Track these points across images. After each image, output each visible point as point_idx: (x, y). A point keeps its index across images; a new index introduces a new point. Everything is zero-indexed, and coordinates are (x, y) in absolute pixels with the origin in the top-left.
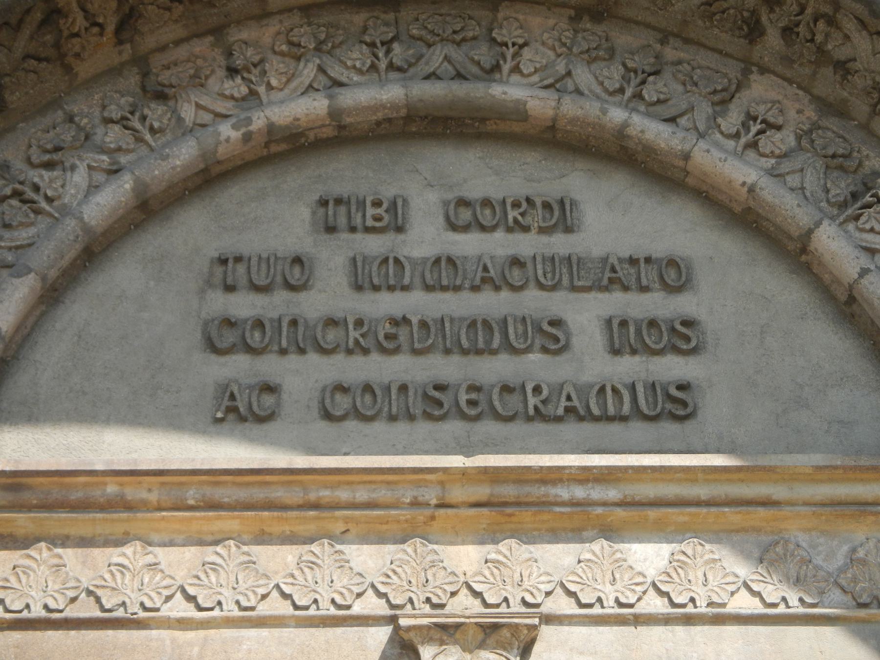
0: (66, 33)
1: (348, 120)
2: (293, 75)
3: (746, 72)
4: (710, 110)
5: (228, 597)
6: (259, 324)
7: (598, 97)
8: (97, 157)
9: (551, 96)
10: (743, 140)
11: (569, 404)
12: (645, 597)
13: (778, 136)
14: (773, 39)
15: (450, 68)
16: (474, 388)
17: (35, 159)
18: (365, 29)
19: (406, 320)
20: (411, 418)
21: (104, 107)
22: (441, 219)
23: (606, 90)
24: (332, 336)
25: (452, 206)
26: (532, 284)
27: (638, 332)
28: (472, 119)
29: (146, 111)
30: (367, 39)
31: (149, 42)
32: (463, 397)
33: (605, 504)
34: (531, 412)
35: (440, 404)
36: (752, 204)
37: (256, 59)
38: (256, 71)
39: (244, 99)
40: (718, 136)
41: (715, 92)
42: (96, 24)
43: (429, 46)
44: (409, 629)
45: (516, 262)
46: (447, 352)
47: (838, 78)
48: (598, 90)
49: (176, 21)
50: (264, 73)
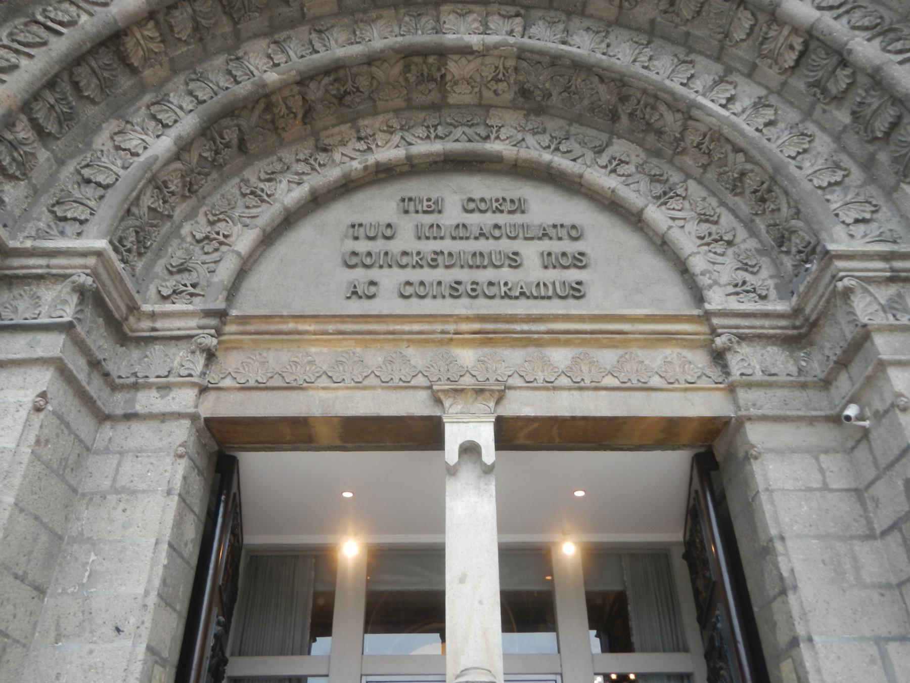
0: (277, 116)
1: (416, 161)
2: (389, 140)
3: (611, 139)
4: (593, 156)
5: (347, 376)
6: (369, 254)
7: (537, 150)
8: (293, 176)
9: (516, 149)
10: (609, 168)
12: (559, 379)
13: (627, 166)
14: (624, 120)
15: (466, 138)
16: (473, 283)
17: (262, 178)
18: (425, 120)
19: (442, 253)
20: (444, 297)
21: (297, 154)
22: (460, 208)
23: (542, 147)
24: (405, 260)
25: (466, 201)
26: (504, 236)
27: (557, 258)
28: (476, 162)
29: (317, 156)
30: (426, 124)
33: (538, 333)
34: (503, 294)
35: (457, 290)
36: (613, 198)
37: (371, 133)
39: (365, 151)
40: (597, 167)
41: (595, 147)
43: (455, 127)
44: (438, 391)
45: (497, 226)
46: (462, 267)
47: (657, 138)
48: (538, 147)
49: (332, 115)
50: (375, 140)
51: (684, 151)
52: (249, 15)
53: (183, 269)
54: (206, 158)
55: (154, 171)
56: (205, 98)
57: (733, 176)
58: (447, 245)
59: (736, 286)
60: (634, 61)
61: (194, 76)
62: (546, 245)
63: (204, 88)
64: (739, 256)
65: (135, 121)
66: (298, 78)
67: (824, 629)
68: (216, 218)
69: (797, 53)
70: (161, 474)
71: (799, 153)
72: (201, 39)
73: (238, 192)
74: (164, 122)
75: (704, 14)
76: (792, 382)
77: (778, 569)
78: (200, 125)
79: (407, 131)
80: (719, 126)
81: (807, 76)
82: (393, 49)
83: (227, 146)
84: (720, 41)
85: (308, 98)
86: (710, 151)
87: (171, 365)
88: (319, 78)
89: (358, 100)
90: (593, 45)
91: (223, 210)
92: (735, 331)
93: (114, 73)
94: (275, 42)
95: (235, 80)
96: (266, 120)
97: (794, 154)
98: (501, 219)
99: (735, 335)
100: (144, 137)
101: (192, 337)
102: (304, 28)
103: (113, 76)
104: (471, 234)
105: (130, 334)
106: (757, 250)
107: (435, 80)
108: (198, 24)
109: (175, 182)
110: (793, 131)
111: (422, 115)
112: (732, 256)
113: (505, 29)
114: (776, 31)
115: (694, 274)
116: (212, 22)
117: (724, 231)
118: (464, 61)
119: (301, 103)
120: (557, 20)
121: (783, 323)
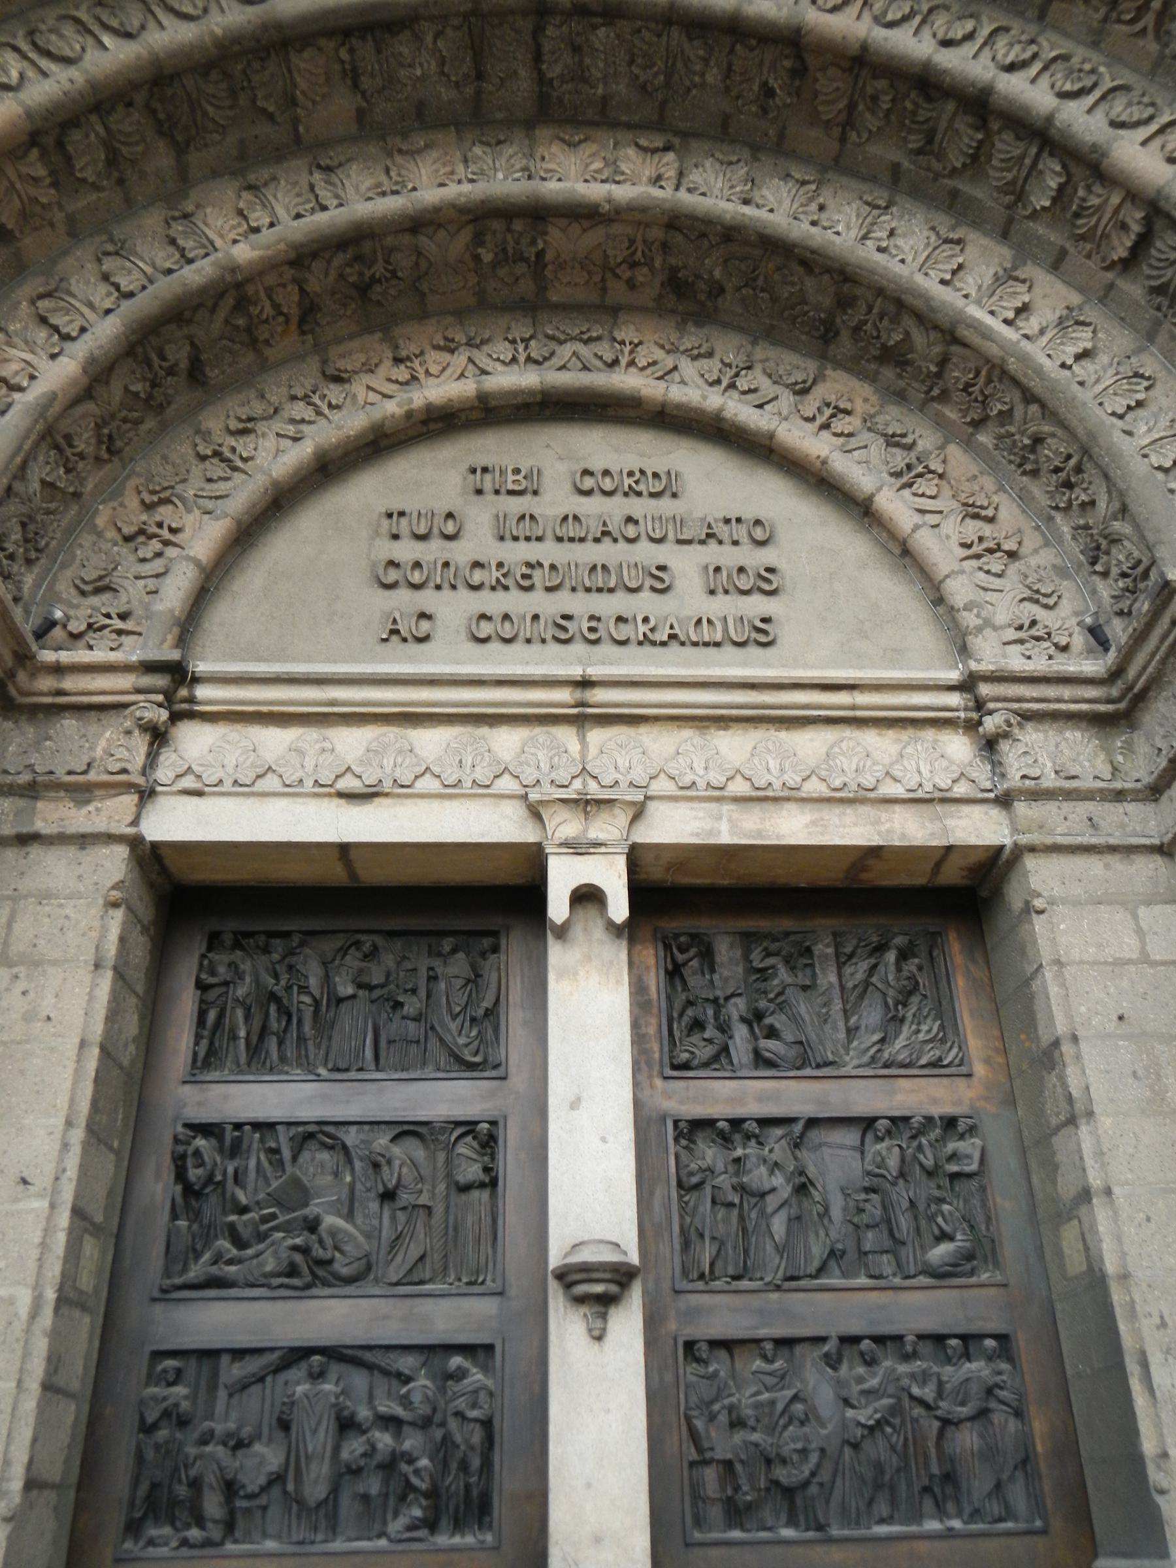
0: (256, 320)
1: (493, 403)
6: (417, 565)
7: (699, 387)
10: (819, 422)
13: (848, 419)
16: (592, 618)
19: (540, 565)
20: (543, 641)
22: (568, 487)
24: (477, 577)
26: (644, 536)
27: (729, 576)
29: (326, 392)
34: (641, 638)
39: (407, 383)
41: (796, 383)
43: (561, 343)
48: (700, 382)
51: (944, 397)
54: (136, 395)
55: (50, 419)
56: (131, 287)
58: (548, 552)
60: (865, 237)
61: (110, 248)
62: (712, 553)
63: (130, 272)
64: (1026, 577)
66: (292, 255)
67: (1130, 1176)
68: (155, 499)
69: (1133, 237)
70: (84, 935)
71: (1129, 408)
72: (121, 182)
73: (190, 451)
74: (64, 330)
75: (982, 159)
76: (1101, 790)
77: (1065, 1085)
78: (127, 337)
79: (478, 347)
80: (1003, 359)
81: (1150, 277)
83: (171, 372)
84: (1008, 207)
85: (308, 289)
86: (986, 397)
88: (327, 255)
90: (795, 206)
91: (166, 484)
92: (1016, 706)
94: (251, 187)
95: (183, 256)
96: (237, 328)
97: (1120, 411)
98: (639, 507)
99: (1016, 712)
100: (28, 356)
101: (125, 706)
102: (299, 162)
105: (21, 700)
106: (1054, 566)
107: (527, 260)
109: (86, 435)
110: (1121, 369)
112: (1015, 578)
114: (1099, 196)
115: (952, 608)
116: (139, 149)
117: (1003, 534)
118: (576, 228)
119: (296, 298)
120: (734, 159)
121: (1092, 692)
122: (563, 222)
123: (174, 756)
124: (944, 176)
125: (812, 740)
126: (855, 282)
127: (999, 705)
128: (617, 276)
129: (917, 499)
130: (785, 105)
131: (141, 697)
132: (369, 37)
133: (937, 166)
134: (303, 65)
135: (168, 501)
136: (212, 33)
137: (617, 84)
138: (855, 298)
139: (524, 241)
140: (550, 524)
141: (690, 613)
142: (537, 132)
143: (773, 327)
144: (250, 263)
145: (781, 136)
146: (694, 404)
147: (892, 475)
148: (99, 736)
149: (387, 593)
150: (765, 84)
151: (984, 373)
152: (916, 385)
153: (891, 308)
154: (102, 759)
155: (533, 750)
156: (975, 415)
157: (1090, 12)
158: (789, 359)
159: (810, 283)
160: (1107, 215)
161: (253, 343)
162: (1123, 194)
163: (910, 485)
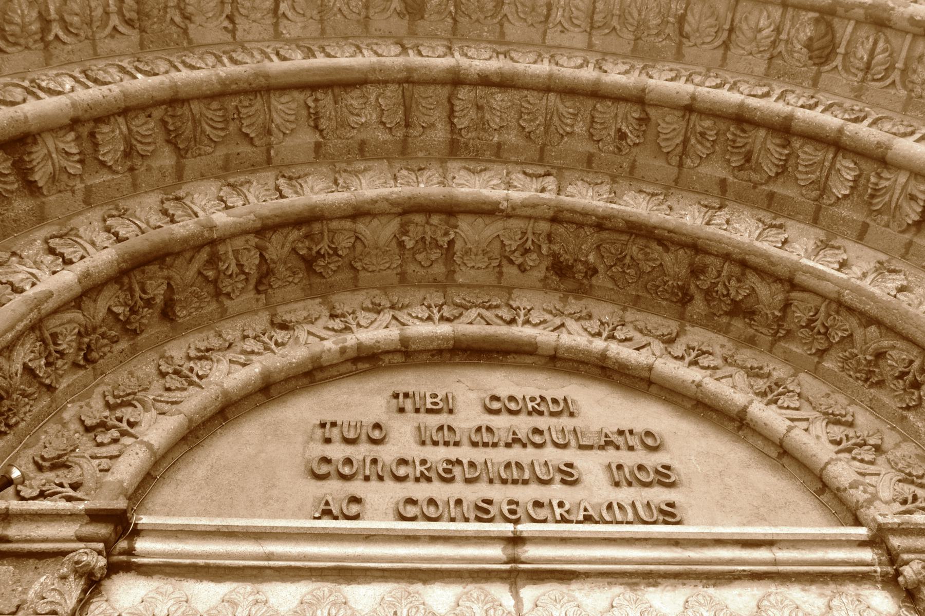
4: (662, 345)
6: (348, 461)
10: (687, 359)
11: (586, 513)
19: (459, 462)
22: (480, 408)
24: (402, 471)
27: (632, 473)
31: (279, 295)
32: (505, 508)
34: (559, 518)
35: (487, 512)
38: (350, 317)
41: (663, 335)
42: (243, 273)
45: (537, 431)
48: (585, 334)
52: (200, 149)
53: (59, 464)
54: (116, 315)
57: (866, 359)
58: (465, 453)
59: (905, 502)
62: (611, 456)
65: (25, 254)
66: (258, 224)
68: (119, 401)
72: (132, 169)
74: (67, 257)
75: (790, 169)
78: (119, 264)
79: (400, 309)
80: (839, 293)
82: (387, 200)
83: (149, 303)
85: (267, 257)
86: (827, 328)
87: (24, 597)
88: (285, 231)
89: (333, 267)
90: (650, 206)
91: (129, 391)
93: (8, 188)
98: (542, 422)
101: (64, 553)
102: (269, 174)
103: (7, 191)
104: (499, 440)
106: (917, 456)
108: (131, 148)
109: (69, 338)
111: (419, 295)
113: (534, 187)
114: (889, 179)
115: (838, 489)
116: (150, 148)
117: (866, 433)
119: (257, 262)
120: (599, 181)
122: (470, 218)
123: (105, 605)
124: (762, 184)
125: (740, 595)
126: (707, 253)
127: (912, 556)
128: (511, 262)
129: (783, 411)
130: (636, 145)
131: (82, 545)
132: (330, 92)
133: (755, 177)
134: (280, 107)
135: (130, 404)
136: (218, 75)
137: (509, 134)
138: (706, 266)
139: (439, 233)
140: (467, 434)
141: (600, 501)
142: (449, 165)
143: (638, 297)
144: (225, 225)
145: (633, 167)
146: (582, 347)
147: (757, 394)
148: (31, 582)
149: (320, 483)
150: (620, 130)
151: (823, 309)
152: (764, 330)
153: (737, 270)
154: (32, 602)
155: (468, 604)
156: (821, 344)
157: (851, 77)
158: (653, 321)
159: (668, 259)
160: (898, 192)
161: (218, 294)
162: (908, 174)
163: (776, 402)
